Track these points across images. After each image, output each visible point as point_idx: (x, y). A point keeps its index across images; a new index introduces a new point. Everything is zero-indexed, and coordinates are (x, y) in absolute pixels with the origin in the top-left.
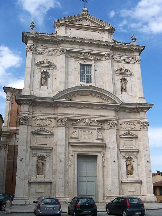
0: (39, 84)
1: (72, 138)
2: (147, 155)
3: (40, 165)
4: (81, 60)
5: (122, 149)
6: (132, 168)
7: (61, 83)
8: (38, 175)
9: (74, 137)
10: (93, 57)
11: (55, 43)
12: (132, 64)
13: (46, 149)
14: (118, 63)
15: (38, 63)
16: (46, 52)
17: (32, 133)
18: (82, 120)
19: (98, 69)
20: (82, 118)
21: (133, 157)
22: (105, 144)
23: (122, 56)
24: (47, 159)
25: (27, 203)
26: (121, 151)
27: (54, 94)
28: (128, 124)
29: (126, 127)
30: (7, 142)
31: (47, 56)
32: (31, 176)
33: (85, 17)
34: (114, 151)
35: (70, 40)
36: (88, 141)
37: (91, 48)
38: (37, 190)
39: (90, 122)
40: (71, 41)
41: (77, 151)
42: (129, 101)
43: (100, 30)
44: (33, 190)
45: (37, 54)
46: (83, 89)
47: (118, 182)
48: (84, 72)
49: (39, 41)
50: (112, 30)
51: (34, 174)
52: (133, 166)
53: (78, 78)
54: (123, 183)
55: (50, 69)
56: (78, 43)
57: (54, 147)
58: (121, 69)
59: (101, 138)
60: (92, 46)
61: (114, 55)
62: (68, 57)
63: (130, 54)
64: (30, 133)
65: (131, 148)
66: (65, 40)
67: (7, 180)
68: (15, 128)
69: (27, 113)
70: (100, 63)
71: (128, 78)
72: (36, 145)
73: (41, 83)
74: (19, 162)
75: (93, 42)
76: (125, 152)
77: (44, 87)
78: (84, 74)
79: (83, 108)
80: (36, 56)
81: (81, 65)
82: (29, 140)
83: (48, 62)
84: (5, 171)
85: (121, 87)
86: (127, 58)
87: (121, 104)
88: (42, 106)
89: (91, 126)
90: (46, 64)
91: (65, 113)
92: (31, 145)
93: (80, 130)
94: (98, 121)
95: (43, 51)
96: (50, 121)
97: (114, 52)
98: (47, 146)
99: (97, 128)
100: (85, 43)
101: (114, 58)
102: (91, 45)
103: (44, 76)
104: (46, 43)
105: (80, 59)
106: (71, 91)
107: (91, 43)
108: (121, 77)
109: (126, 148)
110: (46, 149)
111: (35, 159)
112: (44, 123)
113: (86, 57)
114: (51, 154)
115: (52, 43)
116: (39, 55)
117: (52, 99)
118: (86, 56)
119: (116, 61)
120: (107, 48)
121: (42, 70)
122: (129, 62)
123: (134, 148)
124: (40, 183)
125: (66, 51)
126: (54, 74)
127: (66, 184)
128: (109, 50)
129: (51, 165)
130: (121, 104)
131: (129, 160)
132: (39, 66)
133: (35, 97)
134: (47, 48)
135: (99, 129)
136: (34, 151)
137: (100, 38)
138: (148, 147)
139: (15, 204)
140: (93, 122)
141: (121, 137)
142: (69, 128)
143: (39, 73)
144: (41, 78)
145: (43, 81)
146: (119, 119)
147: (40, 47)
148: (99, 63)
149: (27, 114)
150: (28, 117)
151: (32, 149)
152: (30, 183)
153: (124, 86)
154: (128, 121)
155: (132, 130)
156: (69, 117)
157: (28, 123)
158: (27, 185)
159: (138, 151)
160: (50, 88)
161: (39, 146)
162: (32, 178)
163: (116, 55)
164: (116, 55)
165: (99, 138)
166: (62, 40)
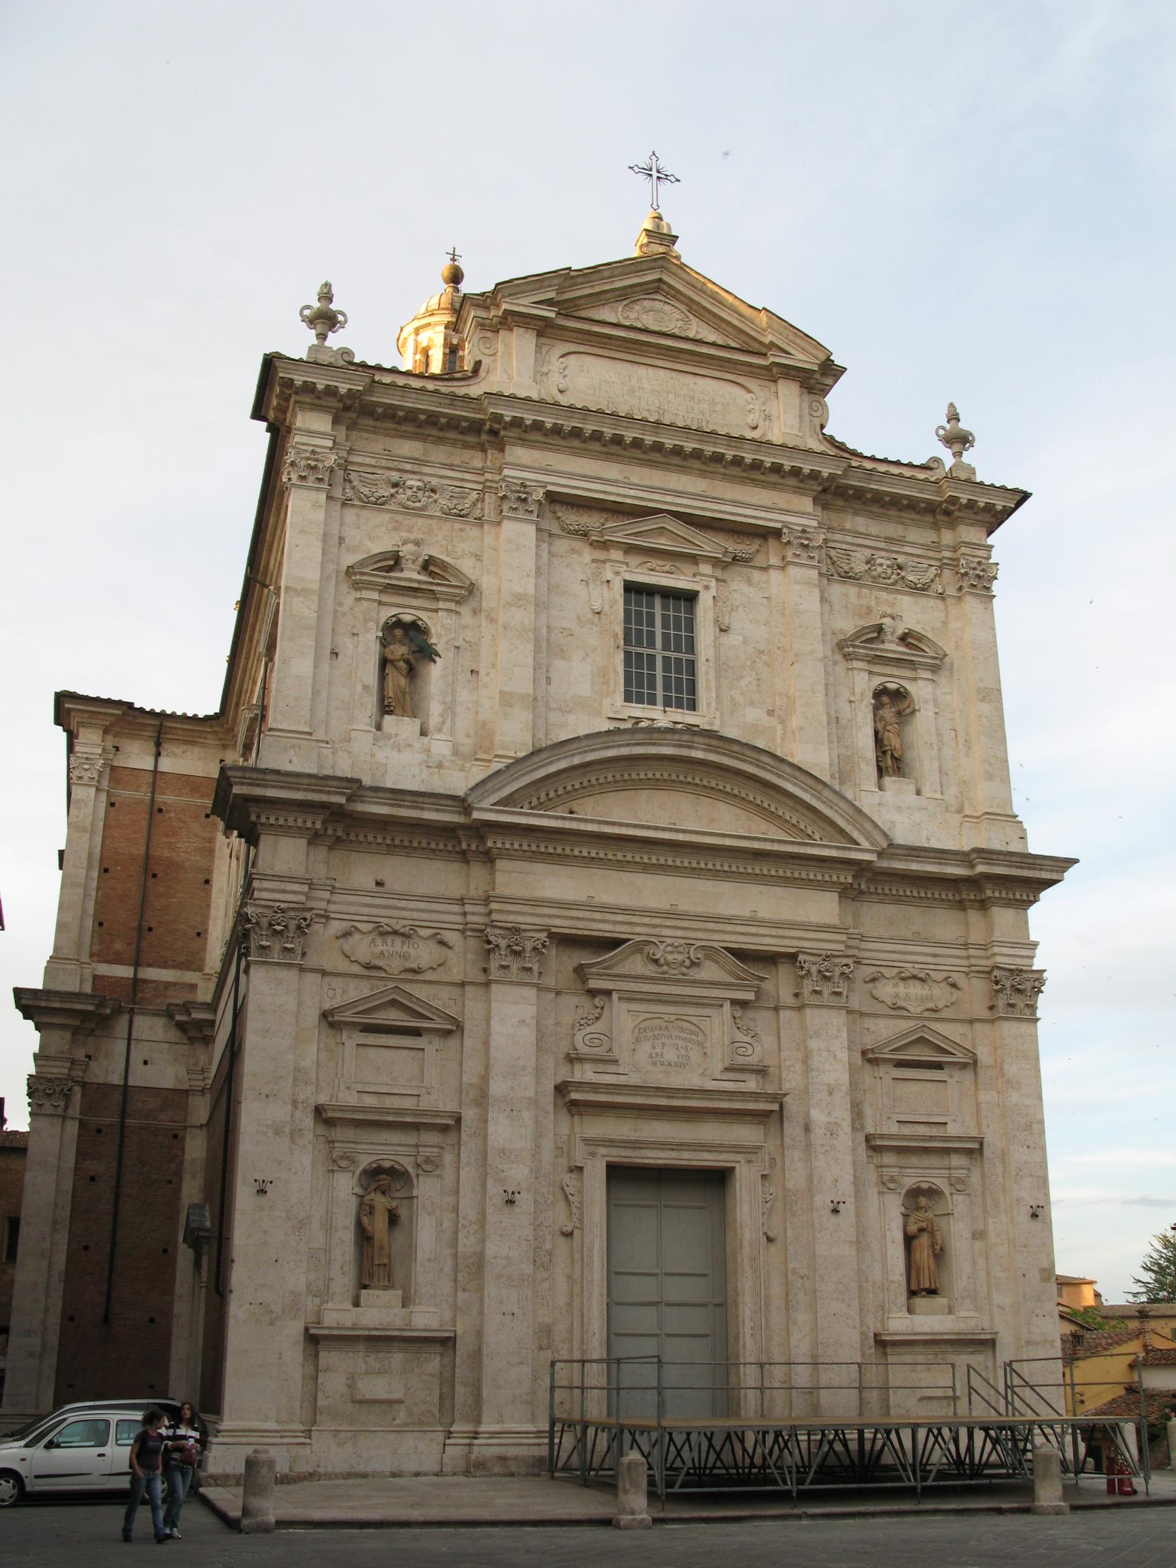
0: (372, 701)
1: (573, 1059)
2: (1030, 1175)
3: (379, 1225)
4: (634, 560)
5: (882, 1137)
6: (940, 1255)
7: (510, 705)
8: (365, 1287)
9: (587, 1050)
10: (709, 544)
11: (471, 439)
12: (942, 596)
13: (416, 1127)
14: (856, 589)
15: (362, 563)
16: (409, 493)
17: (330, 1020)
18: (640, 947)
19: (738, 621)
20: (638, 930)
21: (941, 1184)
22: (778, 1098)
23: (882, 545)
24: (426, 1189)
25: (303, 1468)
26: (874, 1146)
27: (462, 769)
28: (914, 977)
29: (907, 997)
30: (73, 1062)
31: (420, 521)
32: (324, 1293)
33: (660, 280)
34: (833, 1148)
35: (568, 424)
36: (675, 1080)
38: (360, 1384)
39: (688, 963)
40: (576, 433)
41: (610, 1143)
42: (924, 833)
43: (753, 371)
44: (333, 1384)
45: (356, 502)
46: (653, 750)
47: (856, 1338)
48: (652, 635)
49: (369, 422)
50: (824, 374)
51: (343, 1279)
52: (943, 1241)
53: (616, 672)
54: (881, 1343)
55: (441, 605)
56: (614, 449)
57: (470, 1115)
58: (880, 629)
59: (753, 1060)
60: (703, 474)
61: (838, 537)
62: (551, 535)
63: (928, 536)
64: (312, 1016)
65: (934, 1131)
66: (537, 426)
67: (71, 1319)
68: (125, 972)
69: (296, 887)
70: (749, 582)
71: (920, 690)
72: (349, 1098)
73: (382, 698)
74: (243, 1198)
75: (709, 449)
76: (900, 1150)
77: (400, 726)
78: (650, 651)
79: (646, 868)
80: (350, 515)
81: (631, 588)
82: (309, 1062)
83: (428, 565)
84: (61, 1259)
86: (911, 562)
87: (881, 854)
88: (392, 849)
89: (695, 983)
90: (411, 574)
91: (538, 894)
92: (323, 1099)
93: (625, 1006)
94: (741, 955)
95: (395, 485)
96: (442, 943)
97: (834, 518)
98: (425, 1104)
99: (735, 1002)
100: (658, 447)
101: (833, 553)
102: (697, 464)
103: (399, 650)
104: (415, 437)
105: (630, 549)
106: (577, 760)
107: (697, 454)
108: (877, 681)
109: (907, 1130)
110: (416, 1127)
111: (346, 1186)
112: (406, 957)
113: (662, 543)
114: (448, 1158)
115: (453, 435)
116: (365, 513)
117: (462, 804)
118: (661, 534)
119: (847, 577)
120: (797, 490)
121: (386, 614)
123: (953, 1130)
124: (378, 1341)
125: (539, 494)
126: (460, 643)
127: (541, 1348)
128: (806, 504)
129: (446, 1225)
130: (881, 854)
131: (923, 1201)
132: (369, 586)
133: (354, 787)
134: (416, 468)
135: (742, 1004)
136: (339, 1133)
137: (751, 419)
138: (1035, 1126)
139: (227, 1476)
140: (707, 957)
141: (871, 1058)
142: (558, 993)
143: (368, 630)
144: (384, 663)
145: (397, 680)
146: (864, 945)
147: (373, 462)
148: (745, 588)
149: (294, 894)
150: (308, 915)
151: (330, 1123)
152: (314, 1341)
153: (892, 740)
154: (917, 956)
155: (942, 1015)
156: (562, 924)
157: (304, 954)
158: (293, 1354)
159: (975, 1150)
160: (440, 730)
161: (370, 1101)
162: (330, 1305)
163: (849, 539)
164: (849, 539)
165: (741, 1060)
166: (517, 423)
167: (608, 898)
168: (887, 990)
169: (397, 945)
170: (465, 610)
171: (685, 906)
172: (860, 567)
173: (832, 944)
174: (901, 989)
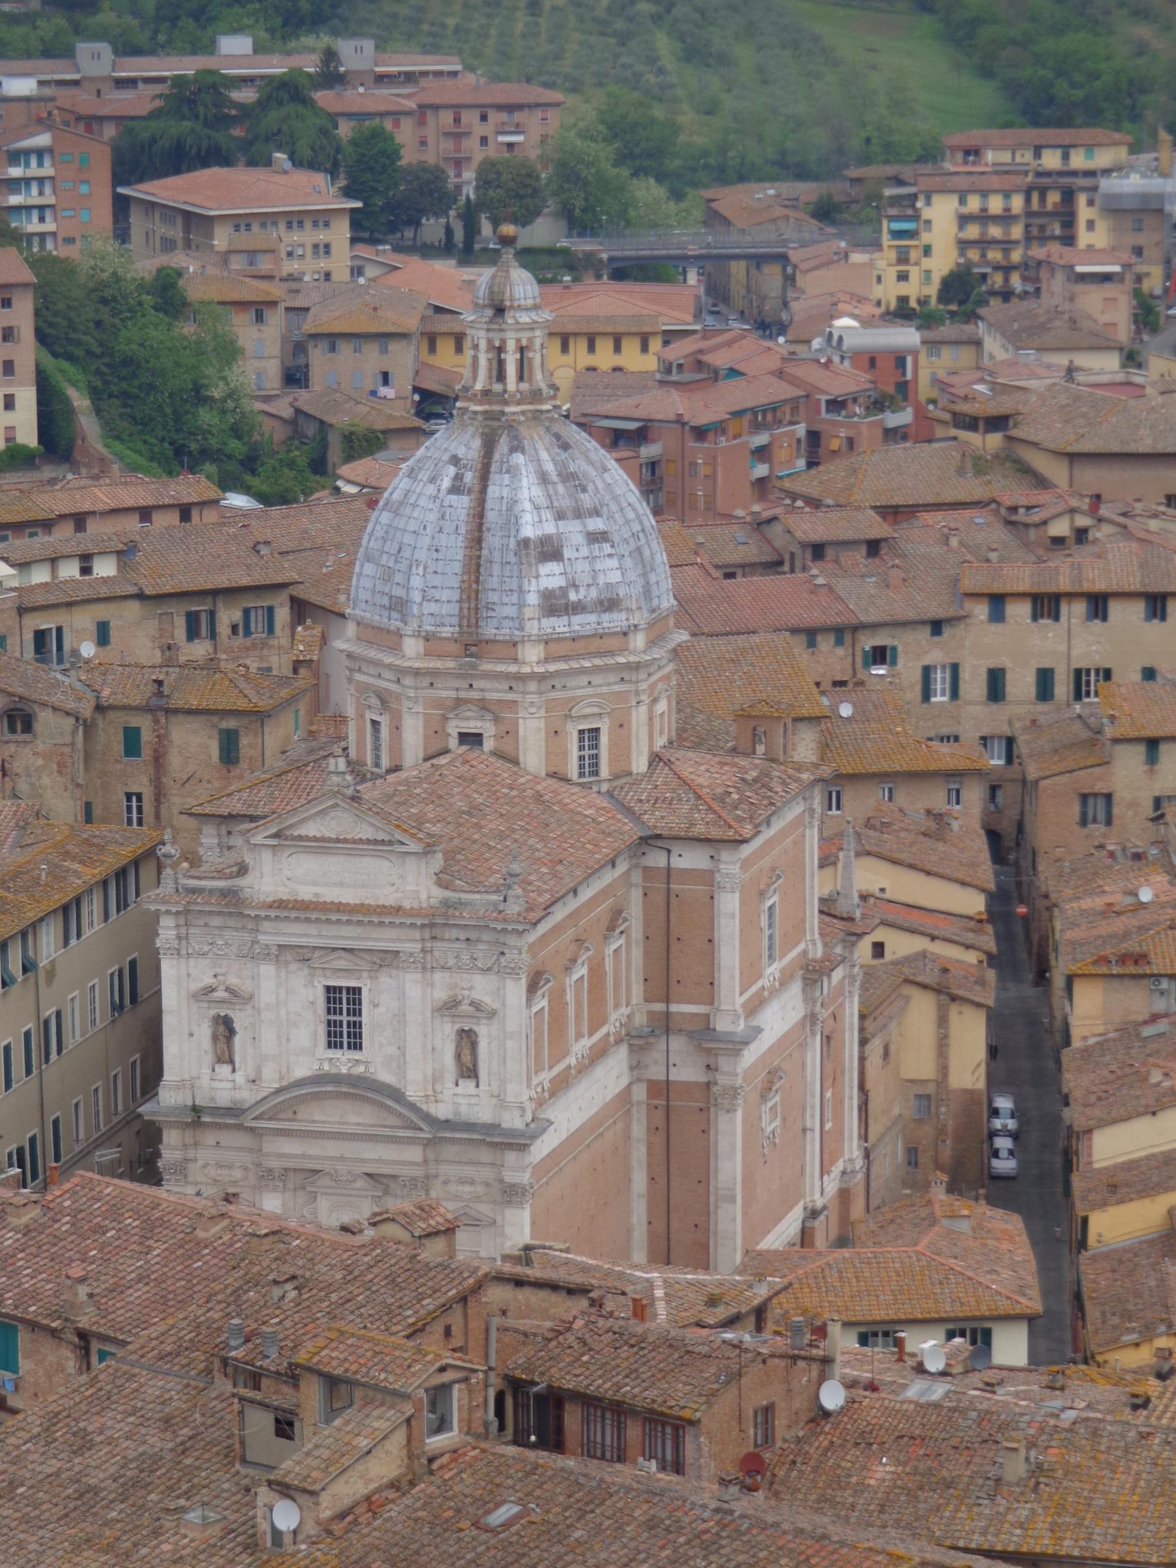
37: (356, 931)
80: (192, 962)
81: (328, 989)
85: (458, 1057)
90: (221, 994)
108: (457, 1026)
121: (213, 1012)
122: (489, 969)
145: (222, 1045)
149: (177, 1155)
156: (290, 1165)
167: (312, 1152)
168: (453, 1188)
169: (225, 1172)
170: (248, 1007)
171: (348, 1155)
172: (451, 962)
173: (418, 1172)
174: (460, 1188)
